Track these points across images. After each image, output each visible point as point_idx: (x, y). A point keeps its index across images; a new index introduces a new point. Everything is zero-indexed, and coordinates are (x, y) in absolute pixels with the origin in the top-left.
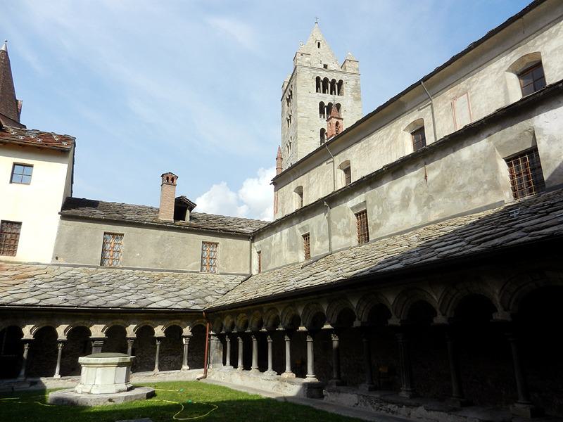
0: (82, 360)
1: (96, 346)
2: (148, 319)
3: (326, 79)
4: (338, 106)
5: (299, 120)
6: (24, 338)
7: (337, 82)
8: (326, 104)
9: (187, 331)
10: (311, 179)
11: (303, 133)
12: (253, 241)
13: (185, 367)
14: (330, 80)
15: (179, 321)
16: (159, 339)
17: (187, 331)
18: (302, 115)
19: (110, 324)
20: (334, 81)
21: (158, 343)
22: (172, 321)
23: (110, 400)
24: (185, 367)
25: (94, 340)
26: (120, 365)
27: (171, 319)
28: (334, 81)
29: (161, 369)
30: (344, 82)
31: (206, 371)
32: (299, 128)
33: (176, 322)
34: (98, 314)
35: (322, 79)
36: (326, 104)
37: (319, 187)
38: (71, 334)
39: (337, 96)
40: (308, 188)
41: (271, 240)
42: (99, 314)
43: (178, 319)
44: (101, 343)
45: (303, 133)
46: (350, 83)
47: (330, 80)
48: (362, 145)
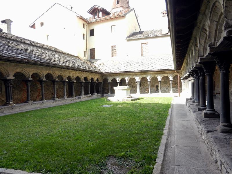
0: (114, 88)
1: (138, 84)
2: (154, 74)
6: (136, 81)
9: (171, 78)
13: (171, 92)
15: (167, 74)
16: (160, 81)
17: (171, 78)
19: (141, 77)
21: (159, 83)
22: (164, 75)
23: (118, 100)
24: (171, 92)
25: (136, 82)
26: (123, 90)
27: (163, 74)
29: (162, 92)
31: (180, 95)
33: (166, 75)
34: (136, 73)
38: (121, 80)
42: (137, 73)
43: (166, 73)
44: (139, 83)
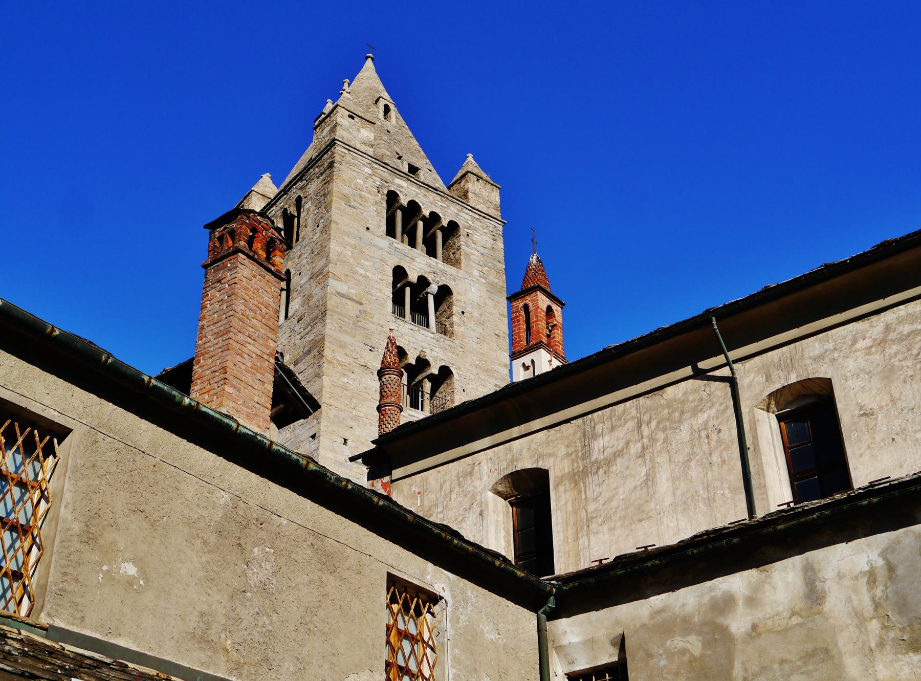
3: (414, 207)
4: (444, 293)
5: (331, 303)
7: (445, 223)
8: (413, 277)
10: (597, 445)
11: (343, 346)
12: (553, 616)
14: (426, 213)
18: (343, 288)
20: (435, 217)
28: (435, 217)
30: (463, 231)
32: (330, 328)
35: (404, 201)
36: (413, 277)
37: (650, 479)
39: (438, 263)
40: (577, 477)
41: (727, 603)
45: (343, 346)
46: (476, 237)
47: (426, 213)
48: (888, 328)
